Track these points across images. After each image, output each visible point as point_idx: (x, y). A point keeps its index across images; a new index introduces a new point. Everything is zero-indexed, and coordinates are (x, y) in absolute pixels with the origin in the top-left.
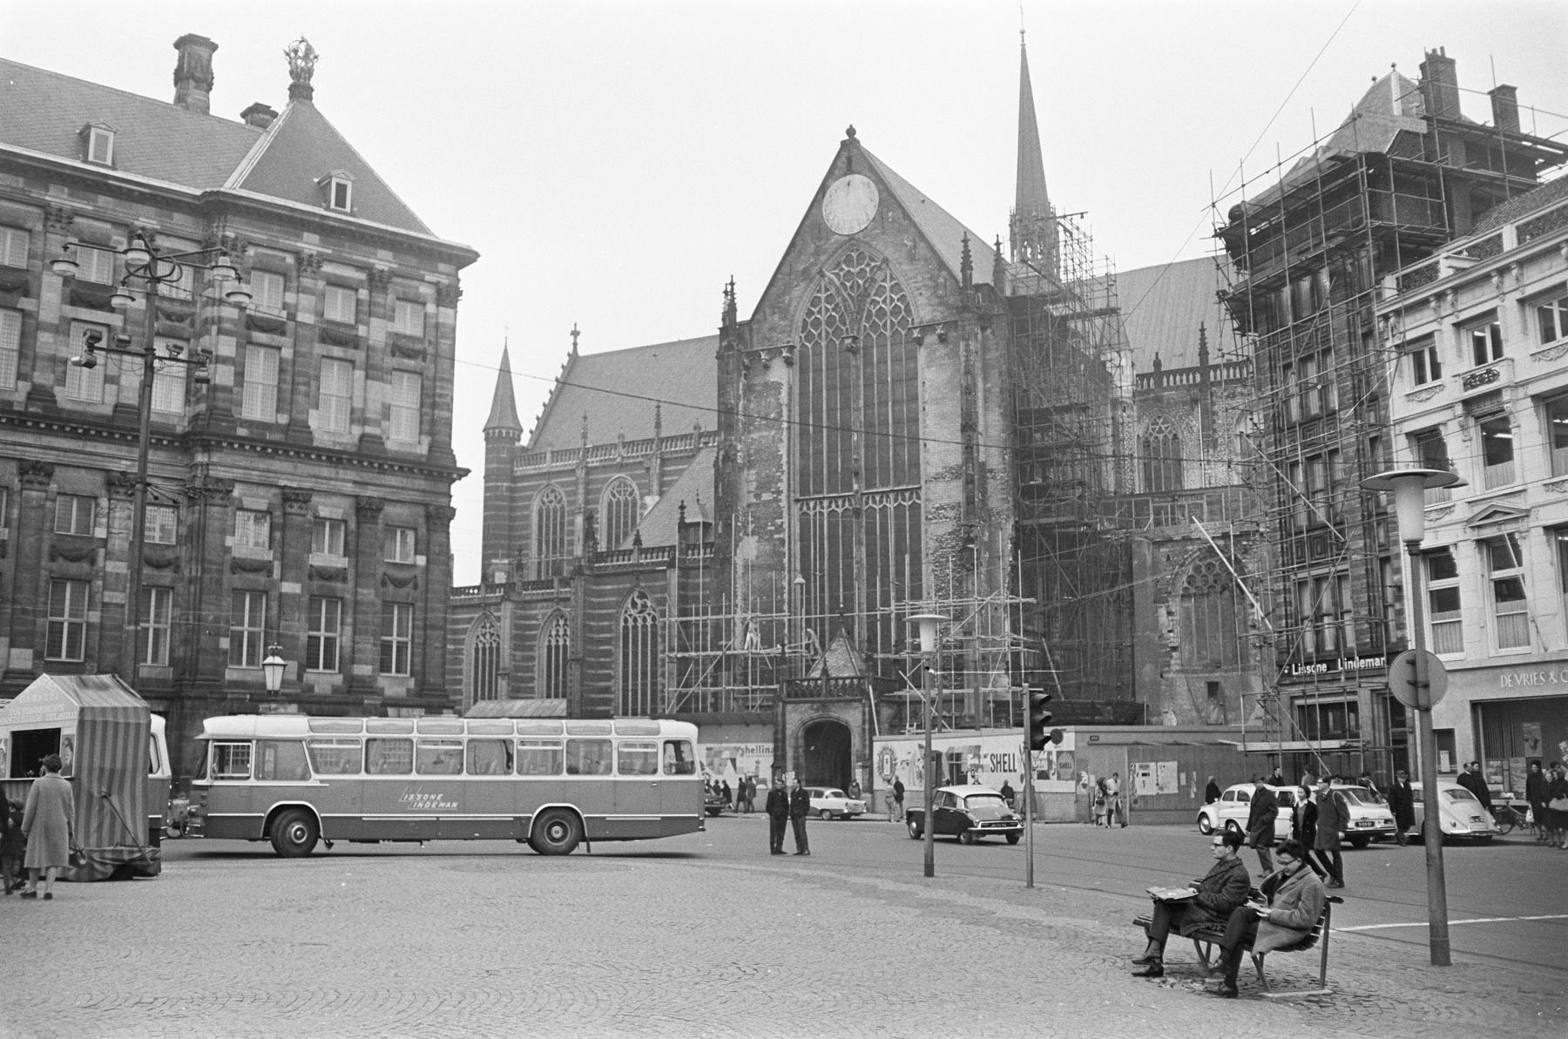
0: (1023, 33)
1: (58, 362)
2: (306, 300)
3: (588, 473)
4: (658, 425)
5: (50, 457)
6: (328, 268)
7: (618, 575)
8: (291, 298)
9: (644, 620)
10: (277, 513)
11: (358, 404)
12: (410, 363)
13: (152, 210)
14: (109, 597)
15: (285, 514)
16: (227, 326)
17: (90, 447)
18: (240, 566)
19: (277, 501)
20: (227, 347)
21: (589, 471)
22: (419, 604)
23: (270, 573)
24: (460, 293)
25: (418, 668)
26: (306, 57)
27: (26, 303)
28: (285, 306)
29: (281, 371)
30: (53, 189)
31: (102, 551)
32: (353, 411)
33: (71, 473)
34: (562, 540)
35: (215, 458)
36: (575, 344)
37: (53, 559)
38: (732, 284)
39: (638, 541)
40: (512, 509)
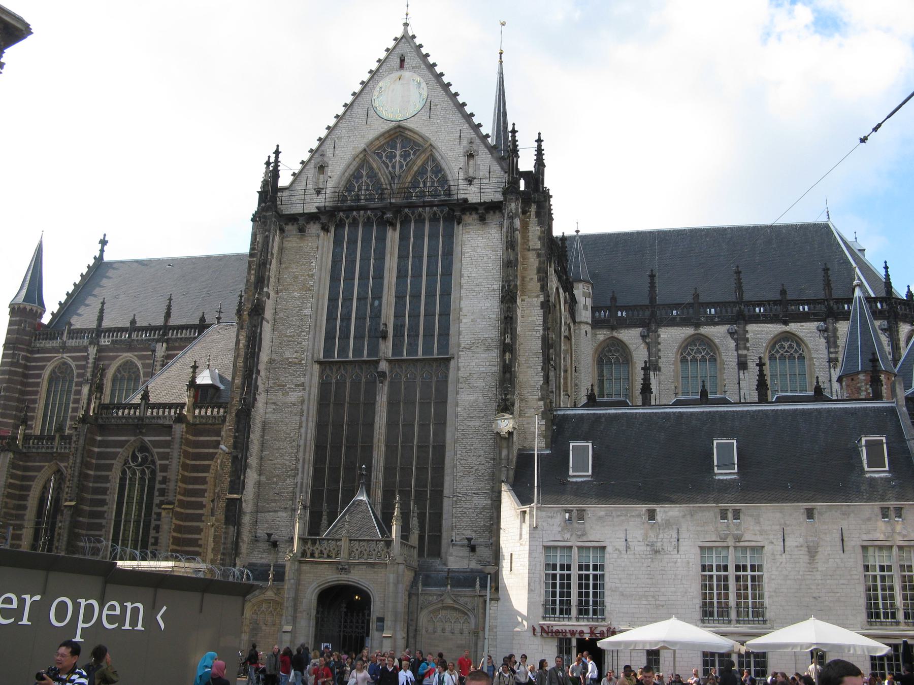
0: (501, 54)
4: (168, 315)
9: (143, 472)
34: (67, 405)
36: (102, 251)
38: (277, 153)
39: (145, 397)
40: (26, 376)
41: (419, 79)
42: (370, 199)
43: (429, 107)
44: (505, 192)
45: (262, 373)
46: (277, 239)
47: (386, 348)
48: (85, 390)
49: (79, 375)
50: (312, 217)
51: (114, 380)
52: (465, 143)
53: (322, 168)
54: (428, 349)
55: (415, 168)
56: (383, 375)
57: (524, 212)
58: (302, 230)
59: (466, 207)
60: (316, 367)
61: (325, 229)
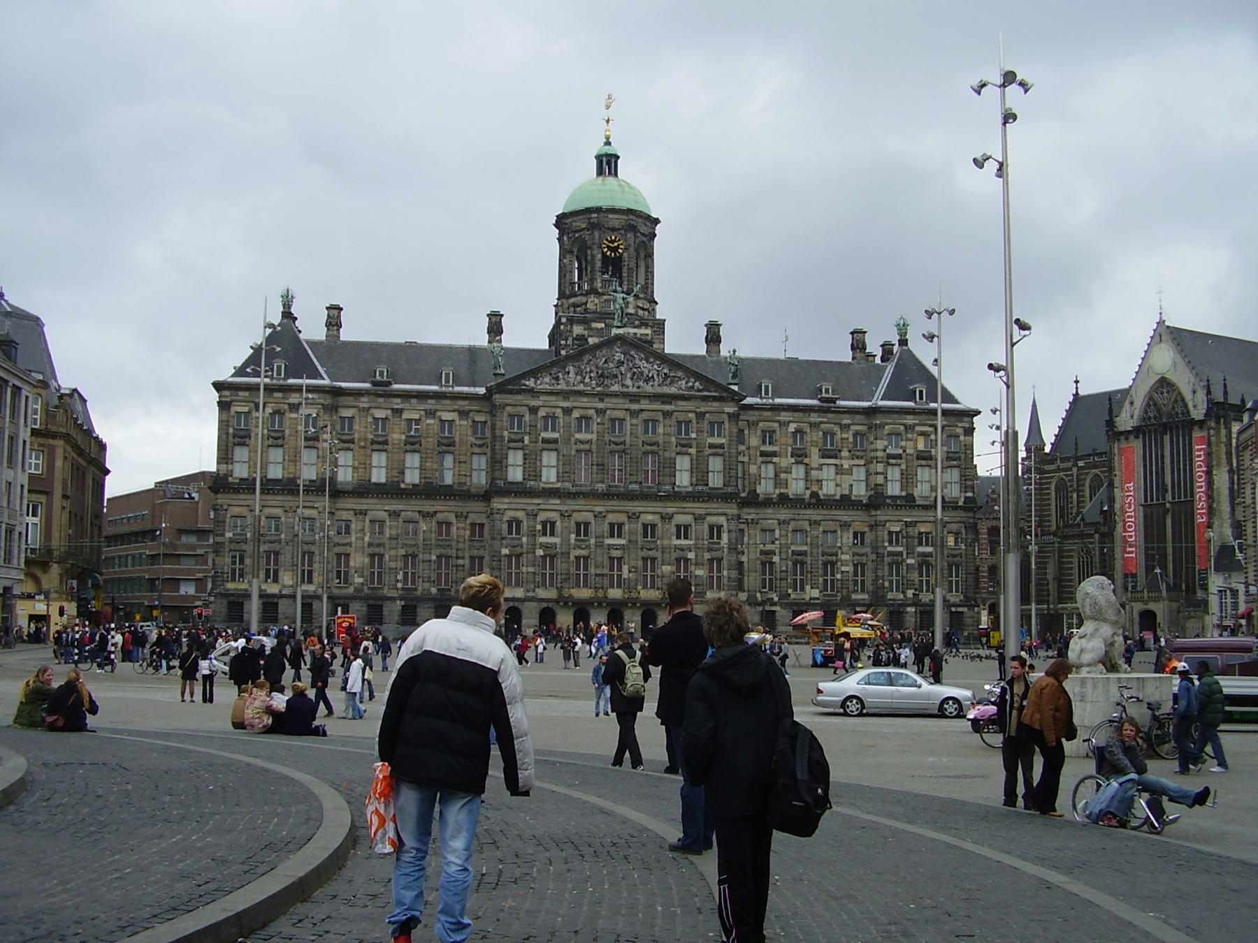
1: (819, 481)
2: (910, 444)
3: (1078, 470)
5: (819, 518)
6: (918, 428)
7: (1074, 537)
8: (903, 443)
10: (904, 532)
11: (934, 484)
12: (955, 462)
13: (847, 416)
14: (843, 569)
15: (907, 532)
16: (879, 460)
17: (834, 512)
18: (890, 554)
19: (904, 527)
20: (880, 468)
21: (1080, 468)
22: (964, 564)
23: (902, 556)
24: (974, 429)
25: (964, 591)
26: (904, 325)
27: (806, 460)
28: (902, 447)
29: (902, 474)
30: (812, 414)
31: (840, 552)
32: (931, 487)
33: (826, 523)
35: (879, 512)
36: (1077, 388)
37: (823, 556)
41: (1168, 347)
42: (1155, 417)
43: (1175, 364)
44: (1206, 415)
45: (1118, 513)
46: (1116, 445)
47: (1169, 497)
48: (1075, 496)
49: (1072, 486)
50: (1129, 431)
51: (1090, 487)
52: (1191, 385)
53: (1132, 403)
54: (1186, 496)
55: (1172, 400)
56: (1168, 510)
57: (1218, 423)
58: (1127, 439)
59: (1193, 423)
60: (1141, 508)
61: (1137, 437)
